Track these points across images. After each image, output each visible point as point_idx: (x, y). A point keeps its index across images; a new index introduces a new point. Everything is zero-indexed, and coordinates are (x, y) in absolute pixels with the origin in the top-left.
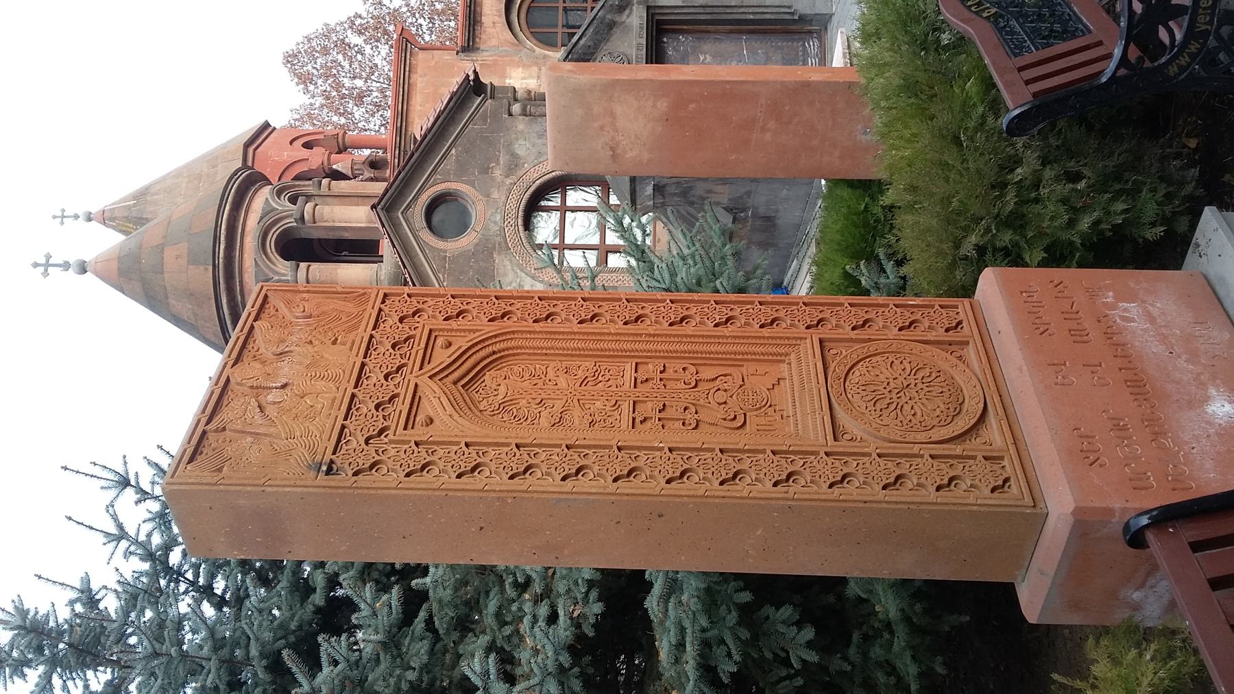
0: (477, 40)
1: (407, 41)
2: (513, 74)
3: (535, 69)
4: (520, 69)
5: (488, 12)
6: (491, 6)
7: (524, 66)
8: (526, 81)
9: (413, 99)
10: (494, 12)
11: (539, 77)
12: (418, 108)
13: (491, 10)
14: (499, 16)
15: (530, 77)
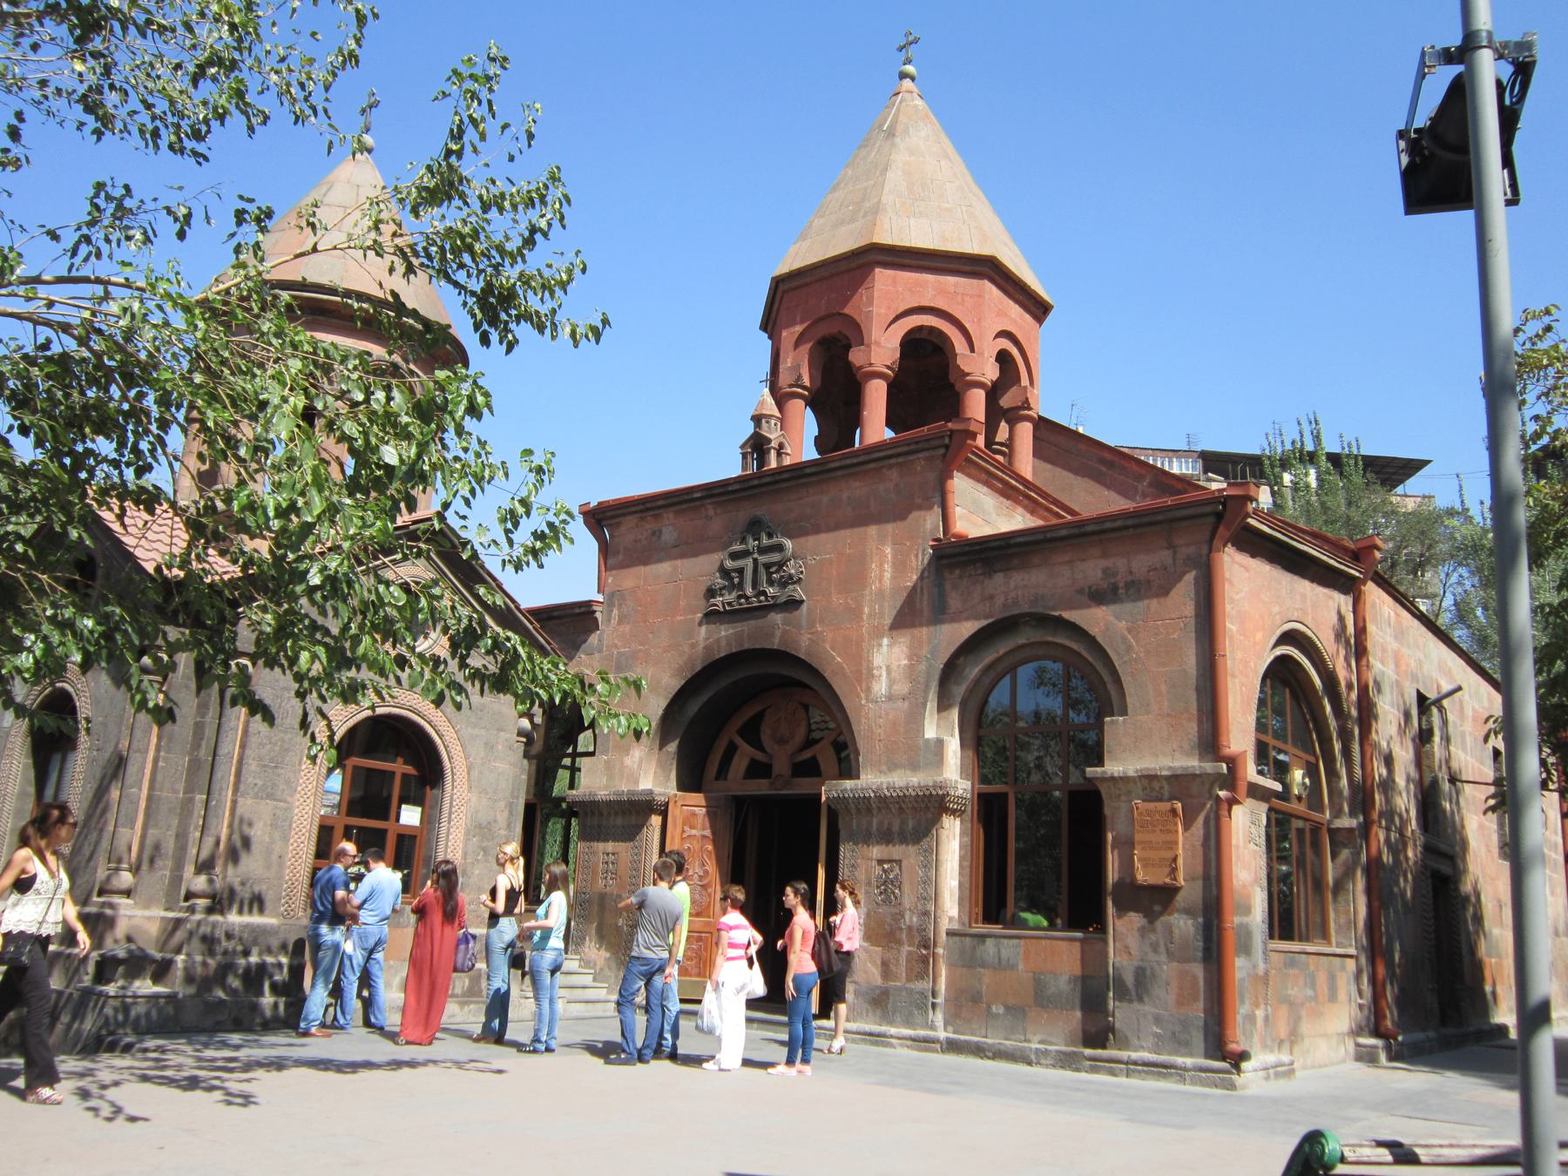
0: (957, 572)
1: (947, 447)
2: (896, 650)
3: (902, 688)
4: (906, 662)
5: (1012, 584)
6: (1026, 586)
7: (911, 668)
8: (884, 674)
9: (857, 484)
10: (1013, 594)
11: (890, 698)
12: (845, 495)
13: (1016, 588)
14: (1005, 606)
15: (891, 682)
